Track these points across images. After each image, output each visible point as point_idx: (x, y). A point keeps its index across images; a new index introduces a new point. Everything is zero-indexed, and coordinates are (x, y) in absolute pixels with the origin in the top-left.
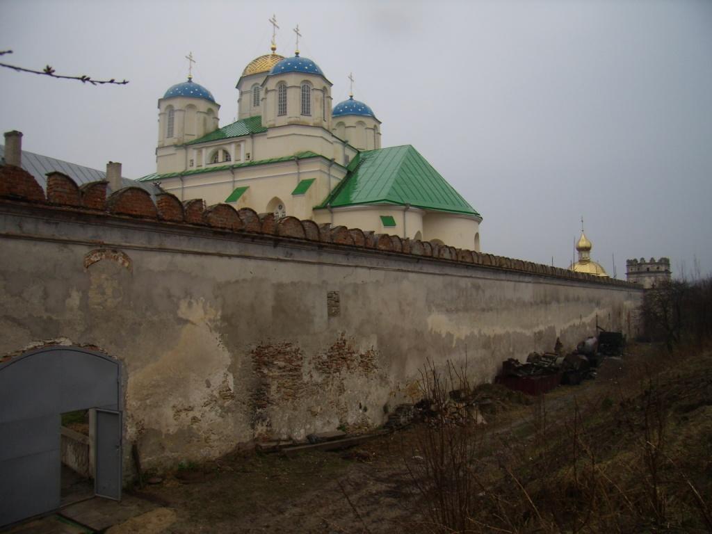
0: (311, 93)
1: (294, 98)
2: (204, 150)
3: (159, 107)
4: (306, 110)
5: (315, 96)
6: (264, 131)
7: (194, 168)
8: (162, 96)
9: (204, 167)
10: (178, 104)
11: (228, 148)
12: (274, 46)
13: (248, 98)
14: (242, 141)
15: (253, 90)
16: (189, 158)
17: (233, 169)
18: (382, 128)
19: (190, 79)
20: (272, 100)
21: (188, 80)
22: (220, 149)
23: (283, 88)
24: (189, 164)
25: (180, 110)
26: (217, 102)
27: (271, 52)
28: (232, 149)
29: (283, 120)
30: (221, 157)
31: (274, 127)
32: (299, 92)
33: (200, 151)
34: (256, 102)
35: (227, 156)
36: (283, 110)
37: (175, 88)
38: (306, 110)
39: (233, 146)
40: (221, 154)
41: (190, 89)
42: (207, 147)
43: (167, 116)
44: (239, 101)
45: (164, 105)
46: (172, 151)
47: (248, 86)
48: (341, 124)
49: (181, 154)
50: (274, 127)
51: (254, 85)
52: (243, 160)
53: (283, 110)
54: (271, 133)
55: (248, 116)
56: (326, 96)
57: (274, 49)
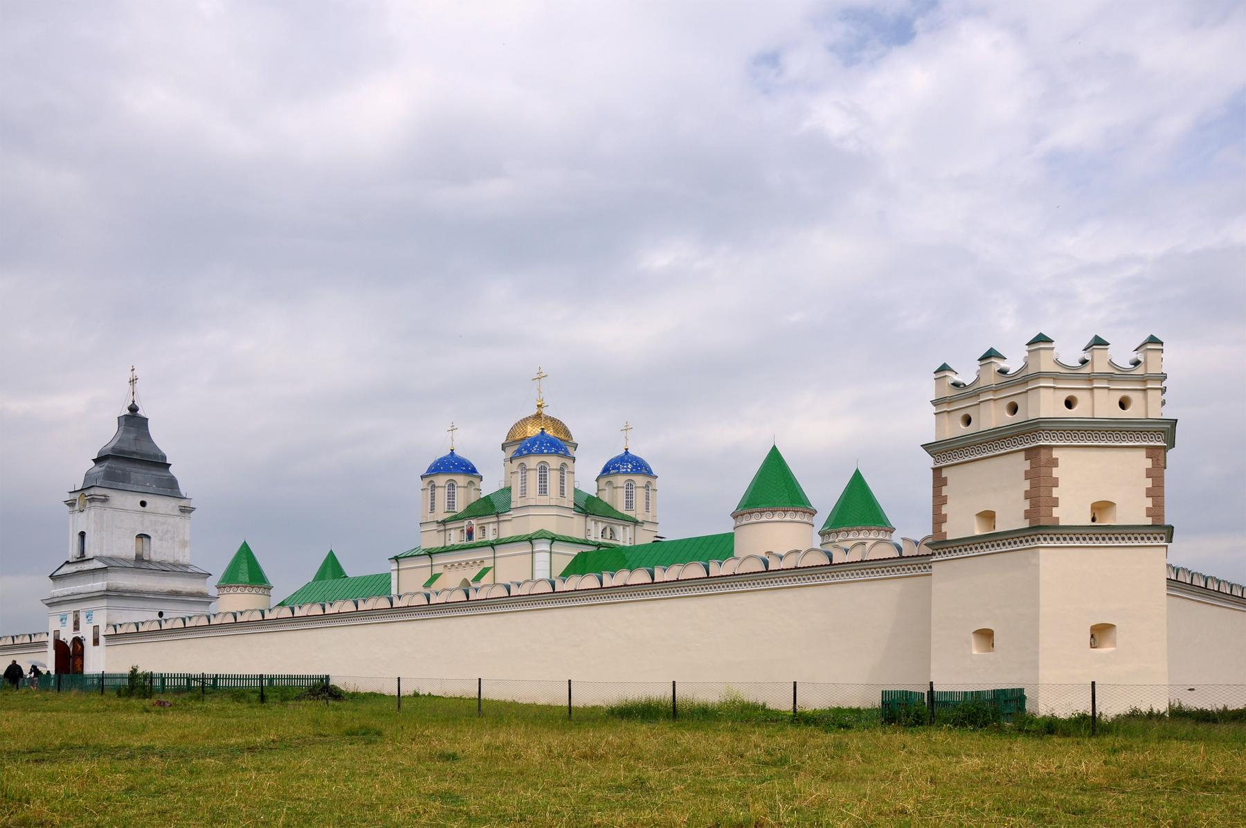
1: (533, 478)
4: (543, 490)
8: (424, 472)
10: (441, 480)
18: (658, 484)
27: (534, 411)
38: (543, 490)
48: (609, 483)
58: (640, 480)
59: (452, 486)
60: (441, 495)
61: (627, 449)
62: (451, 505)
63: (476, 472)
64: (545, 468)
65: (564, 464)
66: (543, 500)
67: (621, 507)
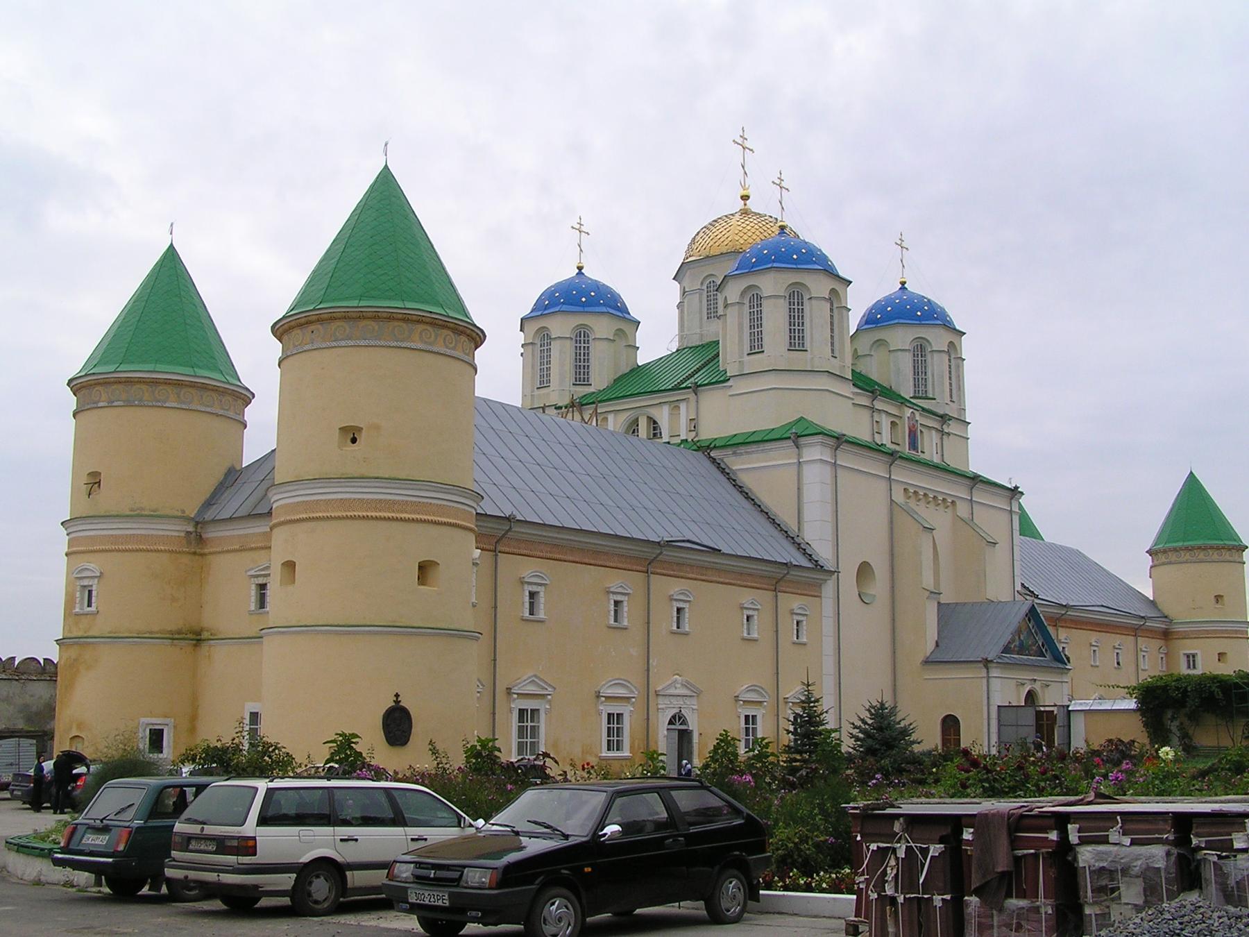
1: (775, 319)
3: (521, 330)
4: (796, 341)
5: (816, 314)
6: (722, 380)
8: (526, 311)
10: (561, 326)
11: (654, 413)
12: (745, 193)
13: (697, 303)
15: (705, 287)
18: (967, 347)
19: (580, 268)
21: (577, 271)
22: (644, 414)
23: (755, 300)
26: (634, 313)
28: (663, 416)
29: (757, 362)
32: (783, 305)
34: (712, 314)
35: (655, 429)
37: (553, 293)
38: (796, 341)
39: (666, 410)
41: (582, 292)
43: (538, 348)
44: (680, 306)
45: (533, 327)
48: (880, 343)
54: (739, 386)
55: (696, 342)
56: (835, 305)
57: (745, 198)
58: (937, 339)
59: (582, 338)
60: (561, 358)
61: (903, 283)
62: (581, 374)
63: (629, 314)
65: (833, 291)
66: (799, 361)
67: (907, 392)
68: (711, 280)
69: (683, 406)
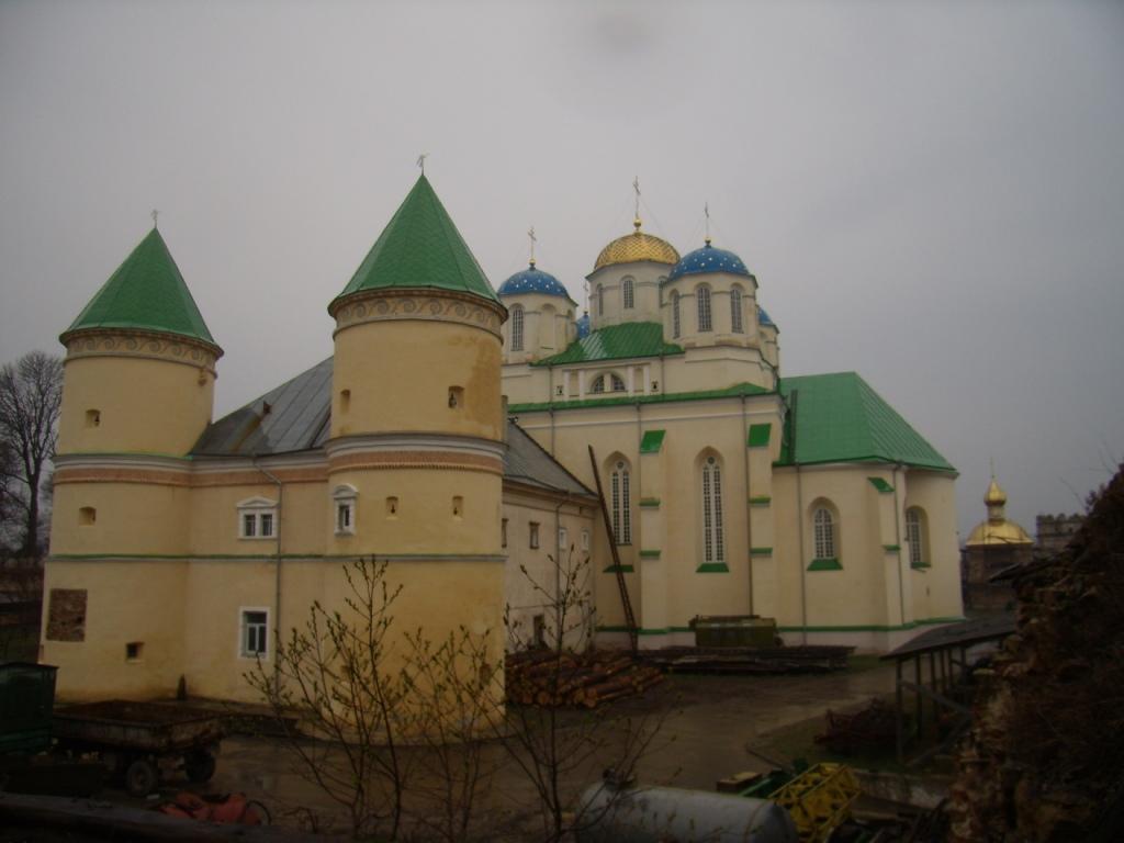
0: (742, 300)
2: (581, 374)
4: (737, 326)
7: (566, 398)
9: (582, 398)
11: (621, 372)
12: (638, 221)
14: (648, 364)
16: (556, 384)
17: (639, 404)
20: (689, 308)
23: (704, 294)
24: (556, 391)
25: (535, 312)
27: (631, 230)
28: (628, 376)
30: (608, 384)
31: (693, 348)
33: (574, 374)
35: (616, 384)
36: (706, 323)
39: (631, 371)
40: (608, 381)
42: (586, 370)
46: (524, 371)
47: (613, 279)
49: (541, 377)
50: (693, 348)
51: (623, 279)
52: (647, 391)
53: (706, 323)
54: (690, 356)
57: (638, 225)
64: (738, 294)
68: (627, 279)
69: (646, 370)
